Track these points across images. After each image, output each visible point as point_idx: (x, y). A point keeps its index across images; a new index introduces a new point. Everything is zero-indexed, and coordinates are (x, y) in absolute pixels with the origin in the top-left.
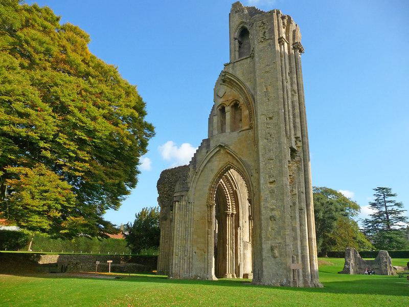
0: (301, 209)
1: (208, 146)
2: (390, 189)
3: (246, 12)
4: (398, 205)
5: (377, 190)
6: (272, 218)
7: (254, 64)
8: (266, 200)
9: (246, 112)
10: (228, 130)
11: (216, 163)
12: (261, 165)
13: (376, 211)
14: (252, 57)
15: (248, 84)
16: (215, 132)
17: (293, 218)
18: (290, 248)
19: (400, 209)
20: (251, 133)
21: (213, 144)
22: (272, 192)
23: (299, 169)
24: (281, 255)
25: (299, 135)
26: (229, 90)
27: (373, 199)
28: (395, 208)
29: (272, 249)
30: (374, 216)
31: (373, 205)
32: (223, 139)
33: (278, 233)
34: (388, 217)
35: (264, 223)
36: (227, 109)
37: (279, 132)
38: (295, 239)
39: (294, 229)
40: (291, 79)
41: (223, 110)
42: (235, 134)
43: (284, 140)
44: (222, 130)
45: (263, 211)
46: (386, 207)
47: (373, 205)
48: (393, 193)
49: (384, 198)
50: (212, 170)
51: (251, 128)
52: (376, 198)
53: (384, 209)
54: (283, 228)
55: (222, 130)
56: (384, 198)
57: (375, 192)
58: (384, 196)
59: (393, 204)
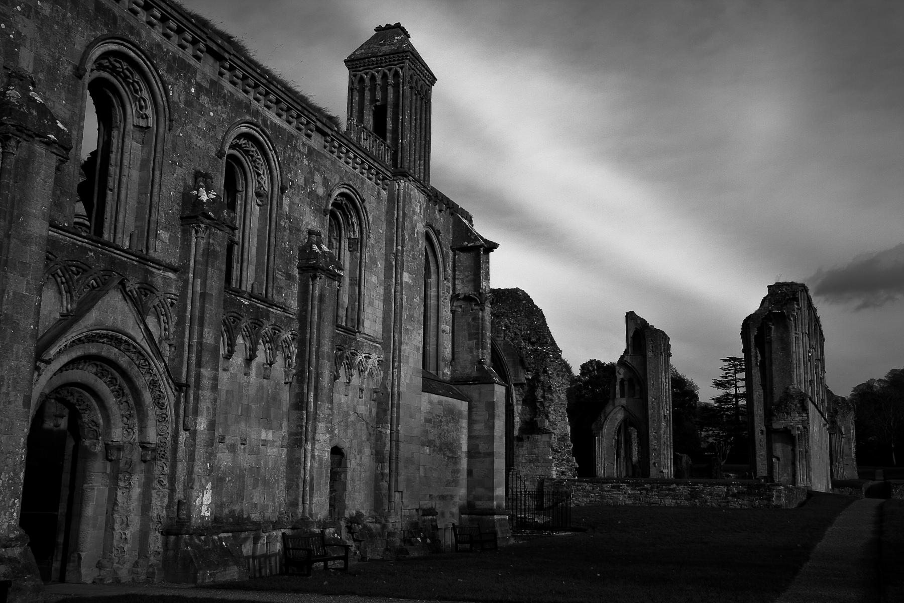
0: (667, 445)
1: (614, 405)
3: (639, 322)
5: (726, 360)
6: (655, 449)
8: (652, 441)
9: (637, 388)
11: (619, 415)
12: (650, 423)
13: (720, 392)
17: (664, 450)
18: (663, 463)
22: (655, 437)
23: (667, 425)
24: (658, 466)
25: (668, 408)
27: (719, 375)
29: (654, 464)
30: (718, 400)
31: (719, 384)
33: (658, 456)
34: (737, 402)
35: (651, 451)
37: (659, 407)
38: (665, 459)
39: (664, 455)
40: (665, 375)
43: (662, 412)
45: (651, 446)
46: (736, 388)
47: (719, 384)
49: (735, 373)
50: (617, 419)
52: (723, 373)
53: (732, 391)
54: (660, 454)
56: (735, 373)
57: (725, 365)
58: (735, 370)
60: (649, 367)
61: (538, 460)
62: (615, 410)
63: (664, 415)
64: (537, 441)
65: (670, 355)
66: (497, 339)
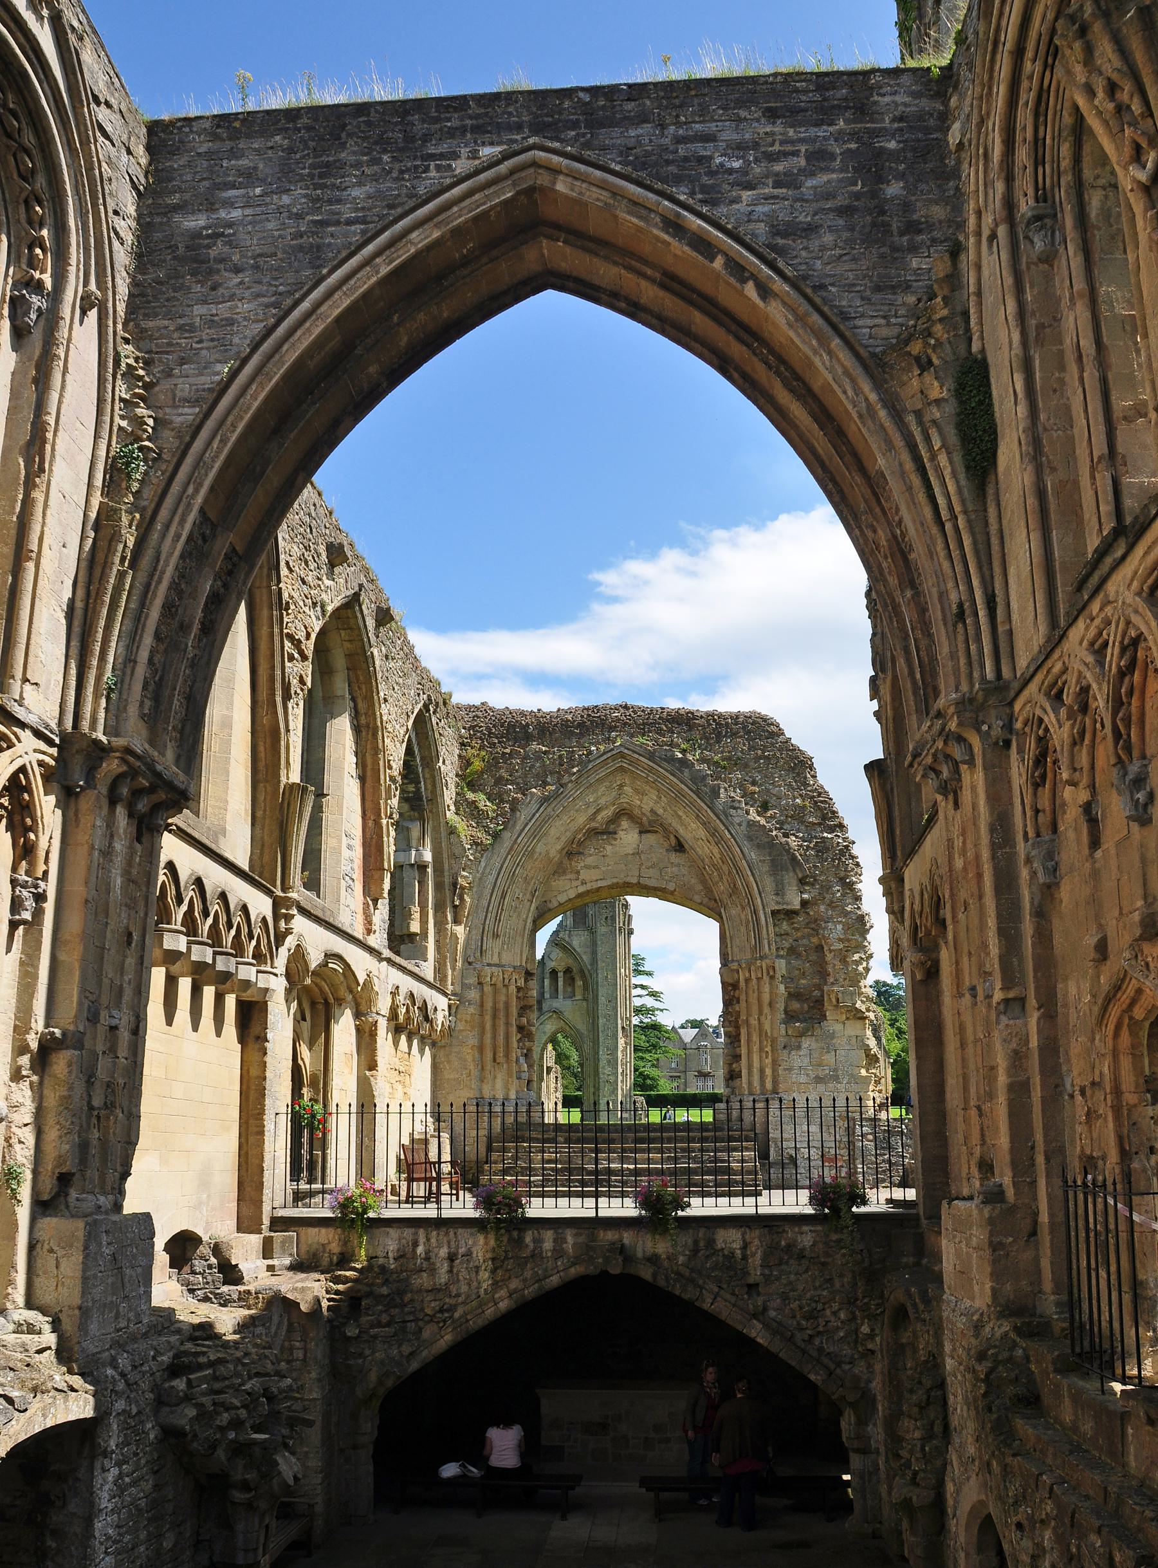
1: (540, 1009)
2: (643, 959)
4: (654, 995)
7: (594, 944)
9: (579, 983)
10: (561, 996)
11: (549, 1027)
14: (592, 931)
15: (584, 957)
16: (547, 996)
19: (657, 1005)
20: (585, 1003)
21: (545, 1007)
22: (609, 1062)
26: (561, 955)
28: (650, 1002)
32: (557, 1004)
35: (602, 1084)
36: (560, 975)
41: (554, 973)
42: (568, 1002)
43: (619, 1022)
44: (555, 994)
48: (646, 968)
51: (584, 999)
55: (555, 994)
59: (644, 992)
60: (601, 950)
61: (836, 1078)
62: (543, 1018)
63: (623, 1028)
64: (832, 1036)
65: (631, 932)
66: (733, 812)
